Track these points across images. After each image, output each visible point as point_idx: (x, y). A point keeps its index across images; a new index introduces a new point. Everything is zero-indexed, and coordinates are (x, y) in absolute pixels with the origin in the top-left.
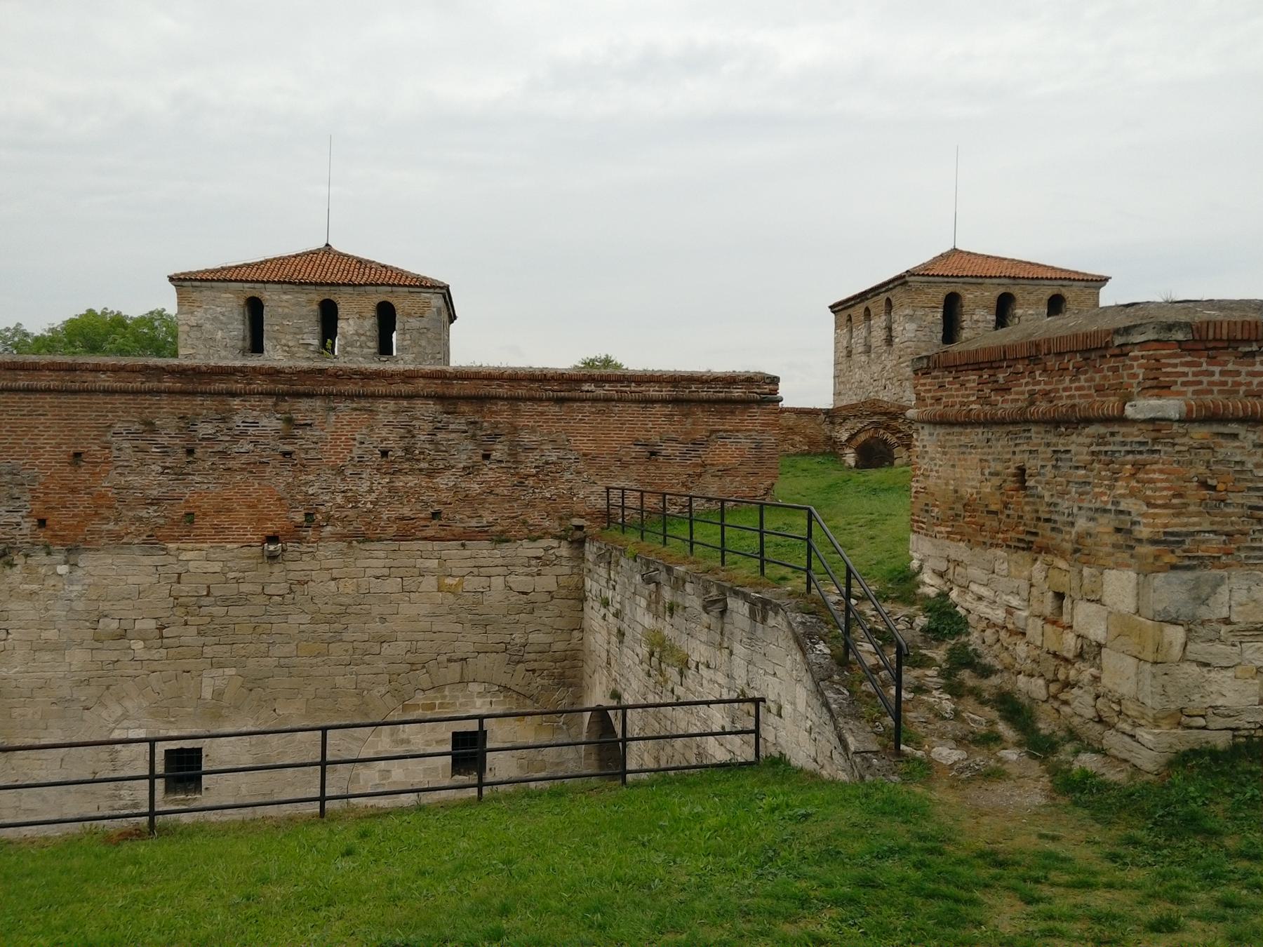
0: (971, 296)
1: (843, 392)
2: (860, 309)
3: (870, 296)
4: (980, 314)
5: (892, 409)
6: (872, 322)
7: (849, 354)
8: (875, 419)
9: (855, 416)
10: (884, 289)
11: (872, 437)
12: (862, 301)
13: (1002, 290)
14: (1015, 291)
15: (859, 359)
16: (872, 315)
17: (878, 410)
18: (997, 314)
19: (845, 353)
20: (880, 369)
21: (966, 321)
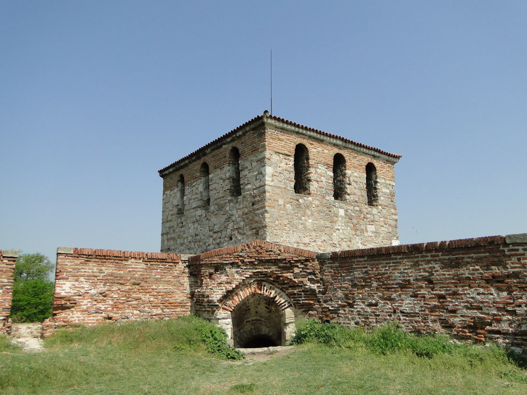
0: (315, 150)
1: (173, 247)
2: (197, 166)
3: (207, 152)
4: (322, 169)
5: (287, 255)
6: (210, 176)
7: (181, 212)
8: (261, 269)
9: (232, 264)
10: (229, 140)
11: (253, 295)
12: (198, 158)
13: (336, 151)
14: (345, 153)
15: (193, 215)
16: (211, 168)
17: (266, 256)
18: (335, 171)
19: (175, 210)
20: (223, 220)
21: (313, 174)
